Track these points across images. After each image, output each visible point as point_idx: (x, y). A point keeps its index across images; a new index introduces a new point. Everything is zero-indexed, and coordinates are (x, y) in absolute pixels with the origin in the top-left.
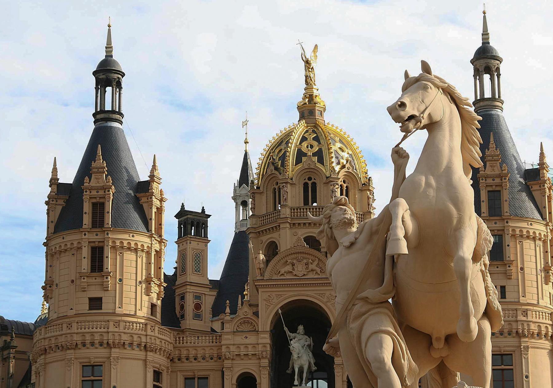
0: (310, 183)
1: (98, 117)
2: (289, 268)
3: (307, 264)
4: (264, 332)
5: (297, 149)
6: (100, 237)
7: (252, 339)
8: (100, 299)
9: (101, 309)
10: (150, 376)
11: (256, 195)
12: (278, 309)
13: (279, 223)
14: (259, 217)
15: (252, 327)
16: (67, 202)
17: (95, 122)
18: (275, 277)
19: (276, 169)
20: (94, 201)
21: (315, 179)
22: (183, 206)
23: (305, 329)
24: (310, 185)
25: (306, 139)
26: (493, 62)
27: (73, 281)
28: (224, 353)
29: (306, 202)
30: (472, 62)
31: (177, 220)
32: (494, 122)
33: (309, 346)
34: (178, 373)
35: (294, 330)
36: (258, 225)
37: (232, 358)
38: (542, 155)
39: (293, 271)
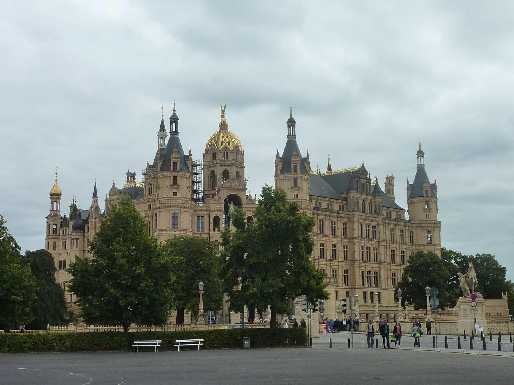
0: (226, 152)
1: (172, 133)
2: (230, 184)
4: (223, 204)
6: (176, 173)
7: (218, 206)
8: (177, 192)
9: (177, 196)
11: (207, 155)
14: (208, 161)
16: (164, 161)
17: (170, 135)
19: (215, 147)
20: (174, 162)
24: (226, 153)
25: (224, 137)
27: (168, 187)
34: (195, 215)
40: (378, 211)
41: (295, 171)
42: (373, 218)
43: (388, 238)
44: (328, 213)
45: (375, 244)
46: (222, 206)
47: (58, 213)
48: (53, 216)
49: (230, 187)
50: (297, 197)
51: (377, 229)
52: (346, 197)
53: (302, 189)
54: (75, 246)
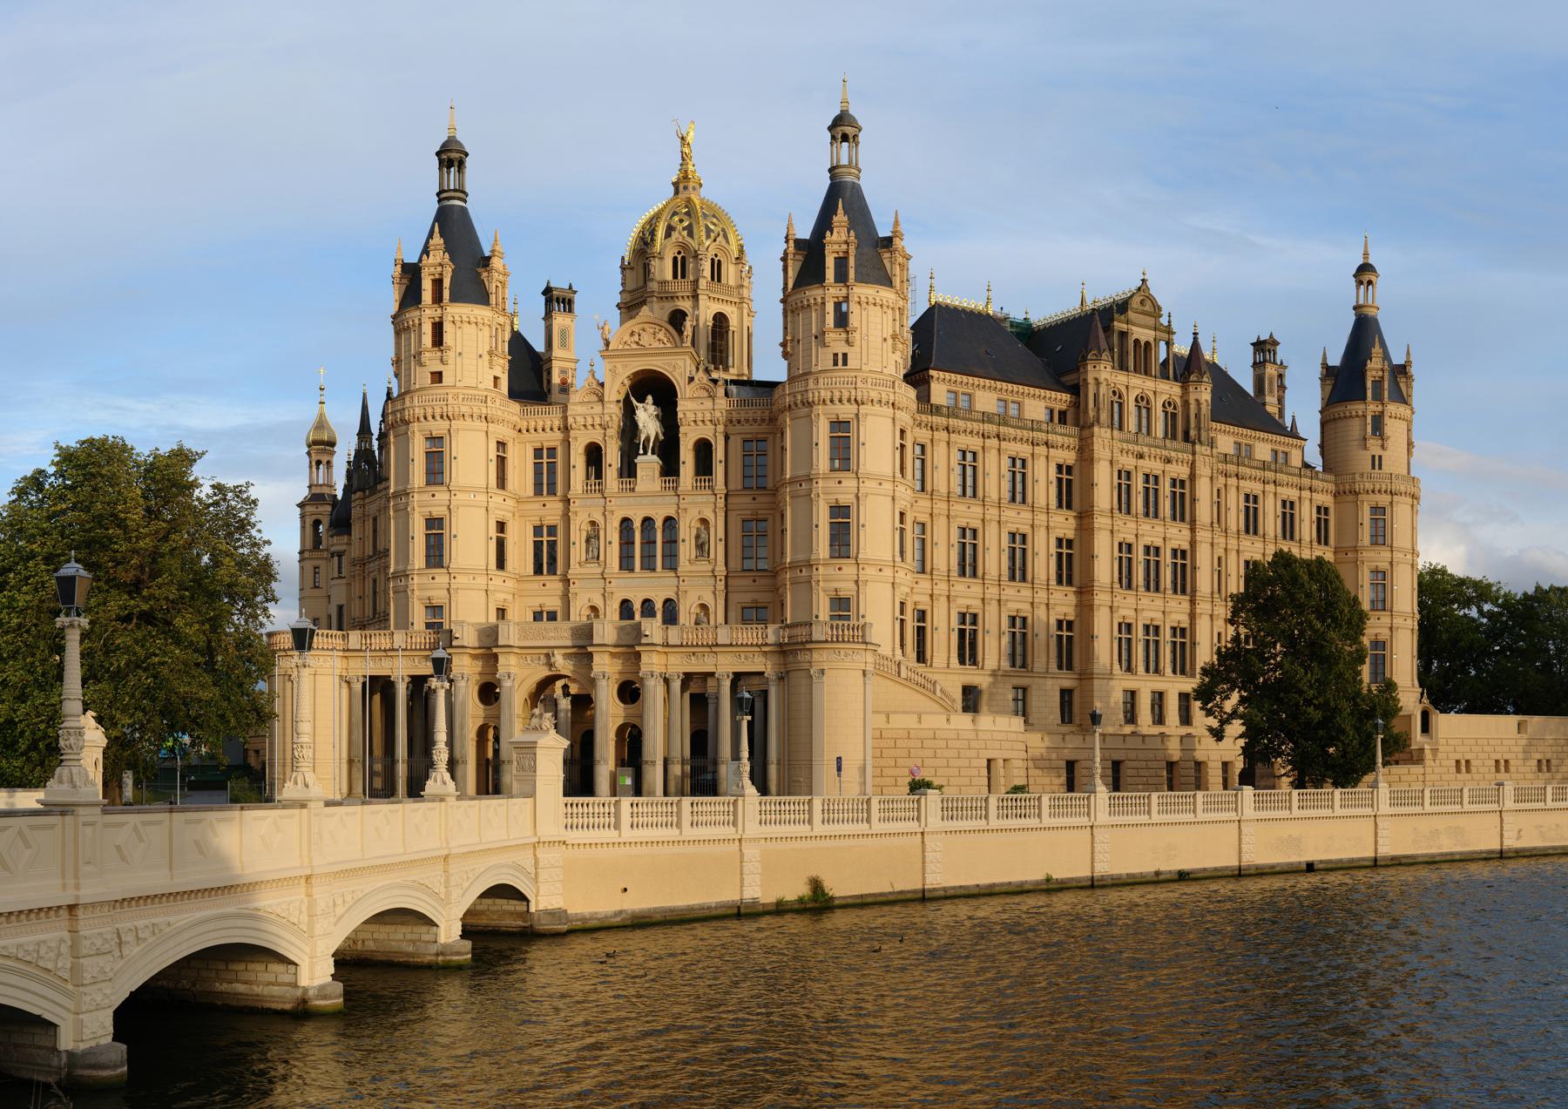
0: (679, 257)
4: (609, 402)
7: (598, 408)
10: (493, 446)
18: (620, 347)
29: (675, 276)
30: (830, 129)
33: (657, 416)
35: (642, 400)
38: (896, 223)
40: (1193, 433)
41: (841, 277)
42: (1173, 454)
43: (1235, 519)
44: (995, 430)
45: (1178, 536)
46: (609, 411)
47: (326, 490)
48: (316, 497)
49: (634, 346)
50: (845, 363)
51: (1187, 491)
52: (1076, 382)
54: (336, 575)
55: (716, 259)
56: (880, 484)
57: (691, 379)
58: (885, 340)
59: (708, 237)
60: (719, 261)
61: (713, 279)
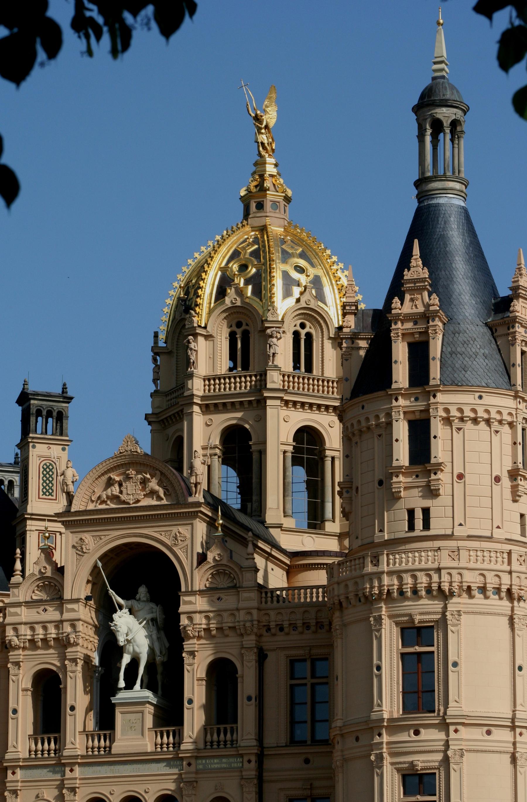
3: (144, 482)
5: (220, 273)
12: (96, 561)
13: (182, 405)
15: (56, 592)
18: (91, 507)
21: (247, 325)
22: (25, 384)
23: (150, 591)
26: (444, 111)
28: (10, 638)
31: (20, 408)
32: (440, 219)
36: (165, 408)
37: (22, 645)
39: (121, 495)
50: (427, 526)
53: (461, 476)
55: (303, 332)
56: (489, 733)
57: (202, 558)
58: (498, 479)
59: (287, 293)
60: (309, 336)
61: (296, 367)
